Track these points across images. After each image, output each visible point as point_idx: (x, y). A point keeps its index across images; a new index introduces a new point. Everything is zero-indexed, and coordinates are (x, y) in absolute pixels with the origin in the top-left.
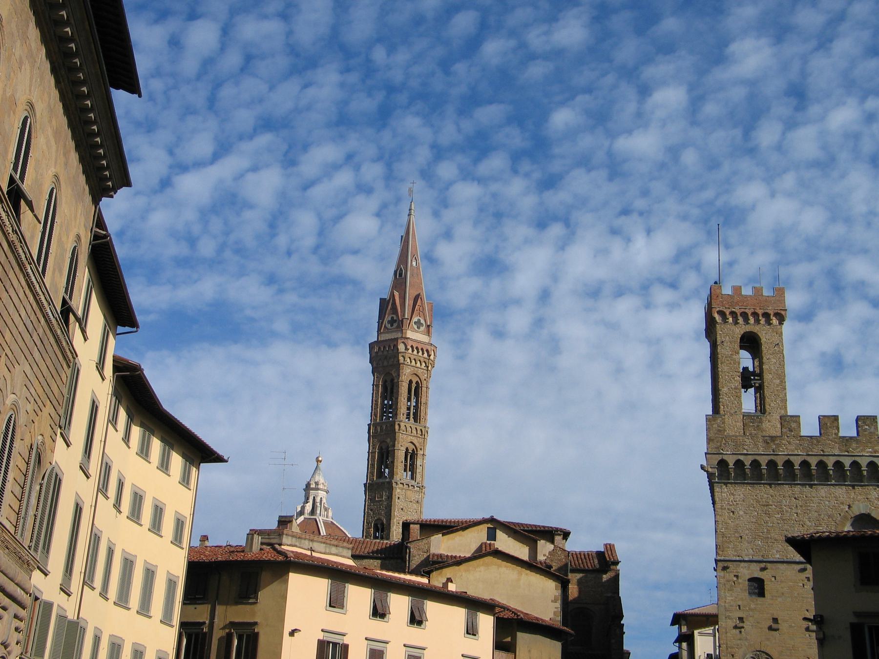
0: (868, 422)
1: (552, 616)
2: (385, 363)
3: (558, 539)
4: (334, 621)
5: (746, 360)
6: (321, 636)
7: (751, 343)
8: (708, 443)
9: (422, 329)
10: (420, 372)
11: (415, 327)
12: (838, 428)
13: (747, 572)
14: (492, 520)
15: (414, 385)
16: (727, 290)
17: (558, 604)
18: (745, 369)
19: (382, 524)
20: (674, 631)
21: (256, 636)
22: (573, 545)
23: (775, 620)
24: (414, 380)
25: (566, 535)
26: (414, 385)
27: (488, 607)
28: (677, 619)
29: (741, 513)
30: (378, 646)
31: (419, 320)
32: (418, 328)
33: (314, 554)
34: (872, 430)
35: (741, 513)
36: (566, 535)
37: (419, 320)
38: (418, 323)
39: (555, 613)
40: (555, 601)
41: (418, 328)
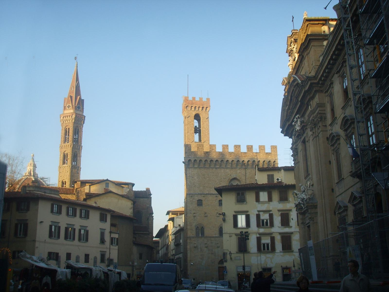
0: (238, 147)
1: (130, 214)
3: (130, 186)
5: (196, 123)
7: (197, 117)
8: (185, 154)
11: (78, 109)
12: (228, 149)
13: (197, 198)
14: (107, 180)
16: (190, 98)
17: (132, 210)
18: (196, 126)
19: (65, 182)
20: (168, 217)
22: (135, 189)
23: (205, 213)
25: (133, 185)
27: (109, 211)
28: (168, 213)
29: (196, 178)
32: (79, 109)
33: (46, 194)
34: (239, 150)
35: (196, 178)
36: (133, 185)
39: (131, 213)
41: (79, 109)
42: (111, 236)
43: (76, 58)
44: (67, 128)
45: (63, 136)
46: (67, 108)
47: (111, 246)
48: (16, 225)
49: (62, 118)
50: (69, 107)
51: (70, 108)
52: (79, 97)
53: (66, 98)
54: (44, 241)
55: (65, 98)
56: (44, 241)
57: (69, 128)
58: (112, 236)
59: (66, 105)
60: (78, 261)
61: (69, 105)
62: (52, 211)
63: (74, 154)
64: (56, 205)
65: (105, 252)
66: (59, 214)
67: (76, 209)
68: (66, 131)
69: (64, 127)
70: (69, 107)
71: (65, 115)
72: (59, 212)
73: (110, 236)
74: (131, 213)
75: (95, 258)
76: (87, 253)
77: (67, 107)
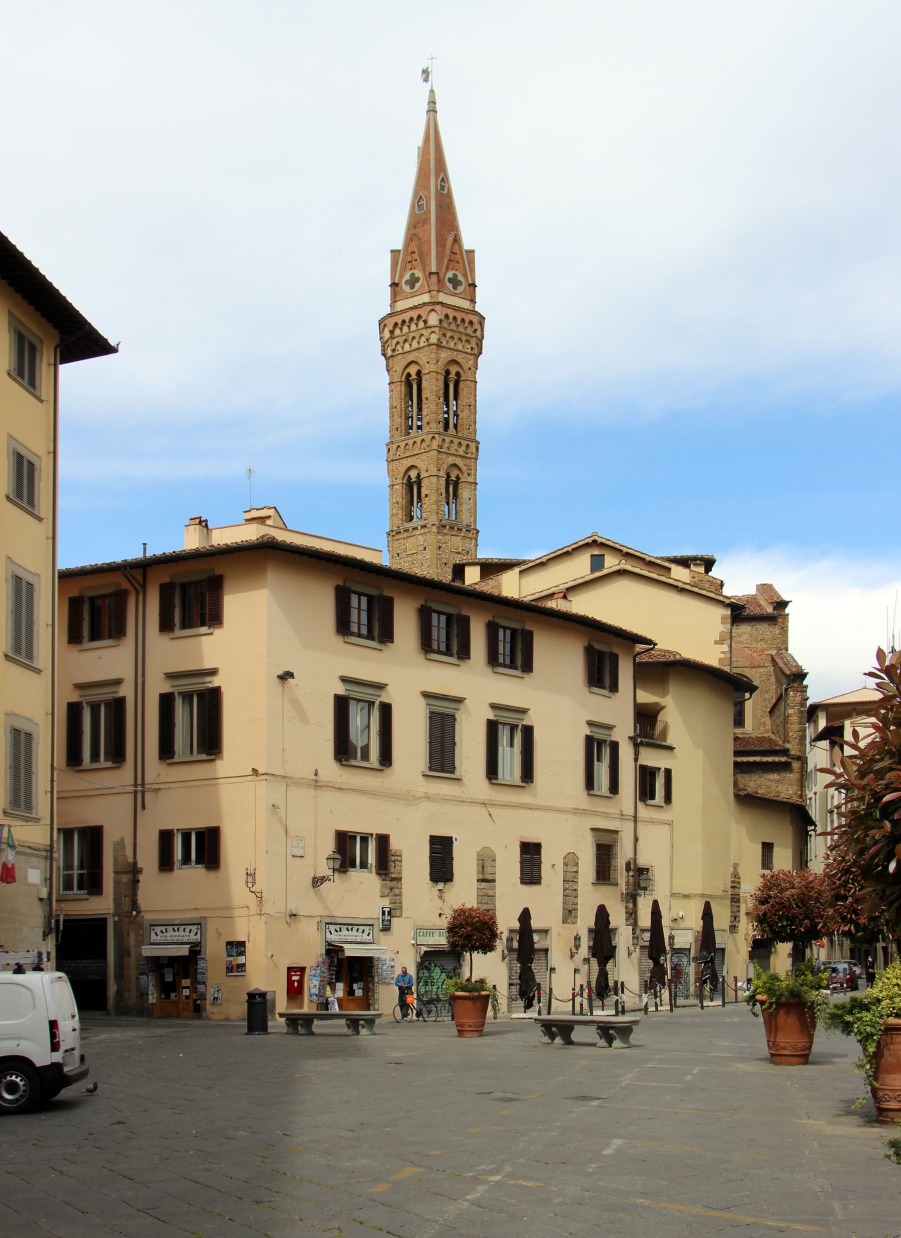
2: (407, 347)
4: (364, 662)
6: (341, 690)
9: (460, 289)
10: (460, 358)
11: (450, 286)
15: (453, 375)
21: (216, 693)
24: (454, 369)
25: (709, 564)
26: (453, 375)
30: (444, 707)
31: (455, 276)
32: (455, 288)
37: (455, 276)
38: (455, 282)
40: (720, 642)
41: (455, 288)
42: (639, 763)
43: (426, 74)
44: (413, 370)
45: (398, 408)
46: (406, 288)
47: (640, 805)
48: (166, 701)
49: (387, 334)
50: (413, 282)
51: (417, 285)
52: (452, 238)
53: (399, 251)
54: (313, 777)
55: (392, 251)
56: (313, 777)
57: (419, 373)
58: (643, 761)
59: (401, 276)
60: (489, 877)
61: (413, 275)
62: (343, 627)
63: (448, 476)
64: (360, 594)
65: (616, 832)
66: (381, 642)
67: (464, 624)
68: (409, 385)
69: (399, 368)
70: (413, 282)
71: (398, 319)
72: (383, 633)
73: (636, 760)
74: (720, 660)
75: (571, 861)
76: (531, 838)
77: (407, 282)
